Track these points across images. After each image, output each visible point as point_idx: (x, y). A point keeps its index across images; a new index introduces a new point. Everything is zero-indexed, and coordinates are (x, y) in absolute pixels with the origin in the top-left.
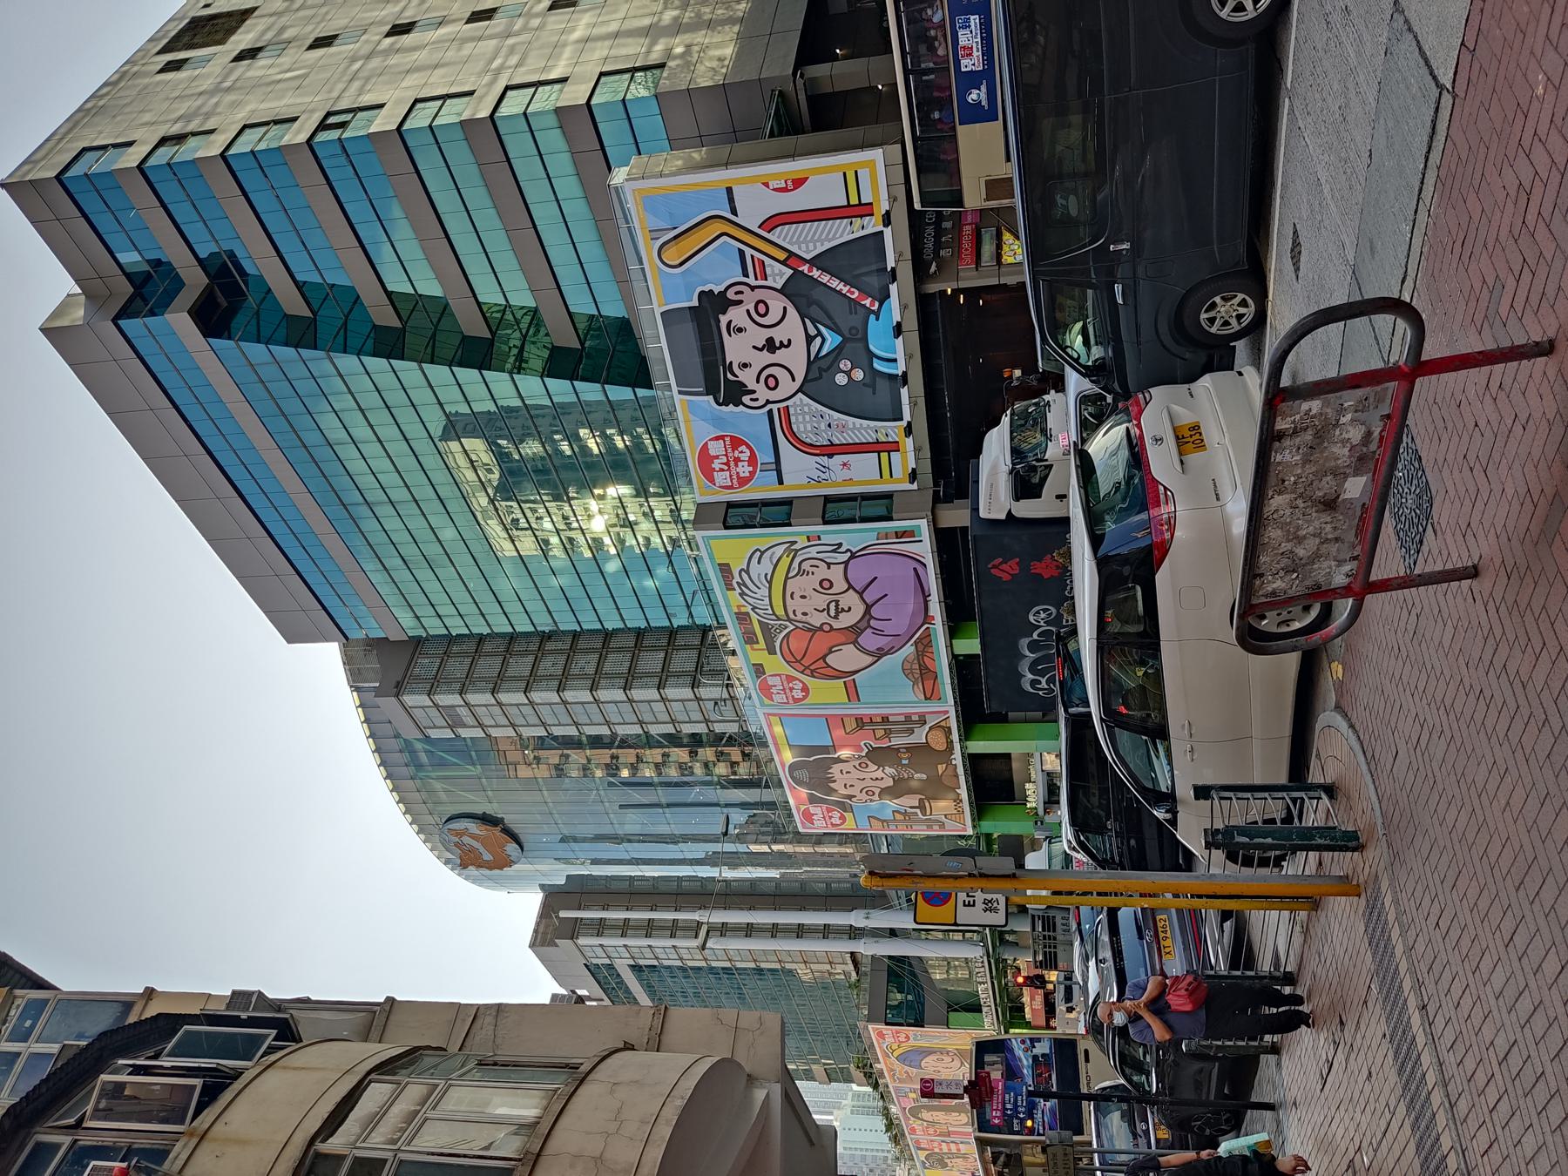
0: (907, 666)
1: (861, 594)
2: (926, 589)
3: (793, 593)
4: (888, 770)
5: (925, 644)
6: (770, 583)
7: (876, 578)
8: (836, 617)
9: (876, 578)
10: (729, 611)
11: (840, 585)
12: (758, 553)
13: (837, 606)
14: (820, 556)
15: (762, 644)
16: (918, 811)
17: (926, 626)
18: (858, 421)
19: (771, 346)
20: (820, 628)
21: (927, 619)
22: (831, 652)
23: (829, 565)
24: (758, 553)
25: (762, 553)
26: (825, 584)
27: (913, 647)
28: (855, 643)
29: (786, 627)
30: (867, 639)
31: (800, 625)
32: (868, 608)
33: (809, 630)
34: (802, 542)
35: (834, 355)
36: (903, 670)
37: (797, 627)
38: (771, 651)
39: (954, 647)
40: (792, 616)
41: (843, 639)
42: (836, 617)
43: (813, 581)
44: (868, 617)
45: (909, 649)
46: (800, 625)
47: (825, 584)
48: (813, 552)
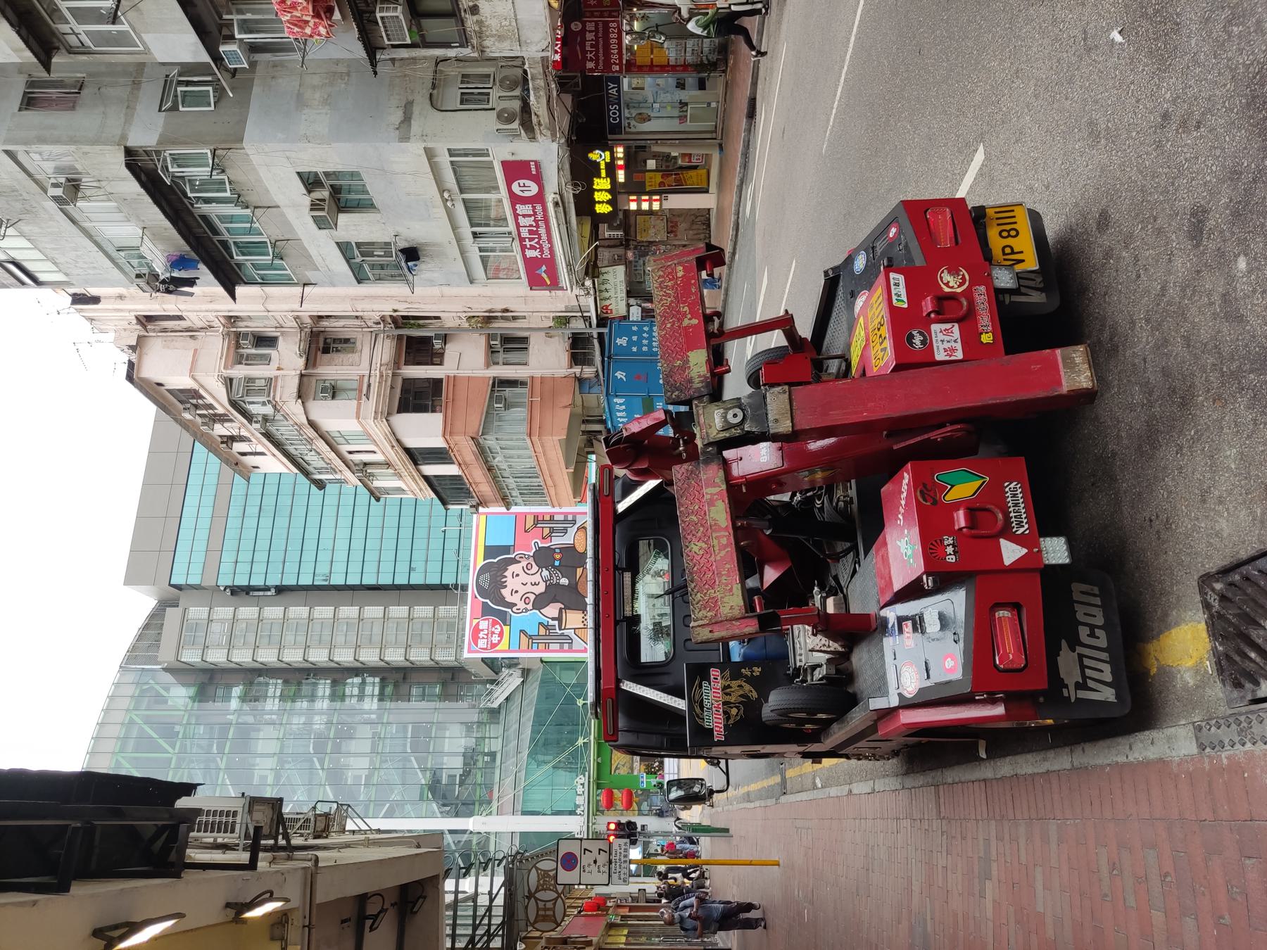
4: (546, 573)
16: (556, 623)
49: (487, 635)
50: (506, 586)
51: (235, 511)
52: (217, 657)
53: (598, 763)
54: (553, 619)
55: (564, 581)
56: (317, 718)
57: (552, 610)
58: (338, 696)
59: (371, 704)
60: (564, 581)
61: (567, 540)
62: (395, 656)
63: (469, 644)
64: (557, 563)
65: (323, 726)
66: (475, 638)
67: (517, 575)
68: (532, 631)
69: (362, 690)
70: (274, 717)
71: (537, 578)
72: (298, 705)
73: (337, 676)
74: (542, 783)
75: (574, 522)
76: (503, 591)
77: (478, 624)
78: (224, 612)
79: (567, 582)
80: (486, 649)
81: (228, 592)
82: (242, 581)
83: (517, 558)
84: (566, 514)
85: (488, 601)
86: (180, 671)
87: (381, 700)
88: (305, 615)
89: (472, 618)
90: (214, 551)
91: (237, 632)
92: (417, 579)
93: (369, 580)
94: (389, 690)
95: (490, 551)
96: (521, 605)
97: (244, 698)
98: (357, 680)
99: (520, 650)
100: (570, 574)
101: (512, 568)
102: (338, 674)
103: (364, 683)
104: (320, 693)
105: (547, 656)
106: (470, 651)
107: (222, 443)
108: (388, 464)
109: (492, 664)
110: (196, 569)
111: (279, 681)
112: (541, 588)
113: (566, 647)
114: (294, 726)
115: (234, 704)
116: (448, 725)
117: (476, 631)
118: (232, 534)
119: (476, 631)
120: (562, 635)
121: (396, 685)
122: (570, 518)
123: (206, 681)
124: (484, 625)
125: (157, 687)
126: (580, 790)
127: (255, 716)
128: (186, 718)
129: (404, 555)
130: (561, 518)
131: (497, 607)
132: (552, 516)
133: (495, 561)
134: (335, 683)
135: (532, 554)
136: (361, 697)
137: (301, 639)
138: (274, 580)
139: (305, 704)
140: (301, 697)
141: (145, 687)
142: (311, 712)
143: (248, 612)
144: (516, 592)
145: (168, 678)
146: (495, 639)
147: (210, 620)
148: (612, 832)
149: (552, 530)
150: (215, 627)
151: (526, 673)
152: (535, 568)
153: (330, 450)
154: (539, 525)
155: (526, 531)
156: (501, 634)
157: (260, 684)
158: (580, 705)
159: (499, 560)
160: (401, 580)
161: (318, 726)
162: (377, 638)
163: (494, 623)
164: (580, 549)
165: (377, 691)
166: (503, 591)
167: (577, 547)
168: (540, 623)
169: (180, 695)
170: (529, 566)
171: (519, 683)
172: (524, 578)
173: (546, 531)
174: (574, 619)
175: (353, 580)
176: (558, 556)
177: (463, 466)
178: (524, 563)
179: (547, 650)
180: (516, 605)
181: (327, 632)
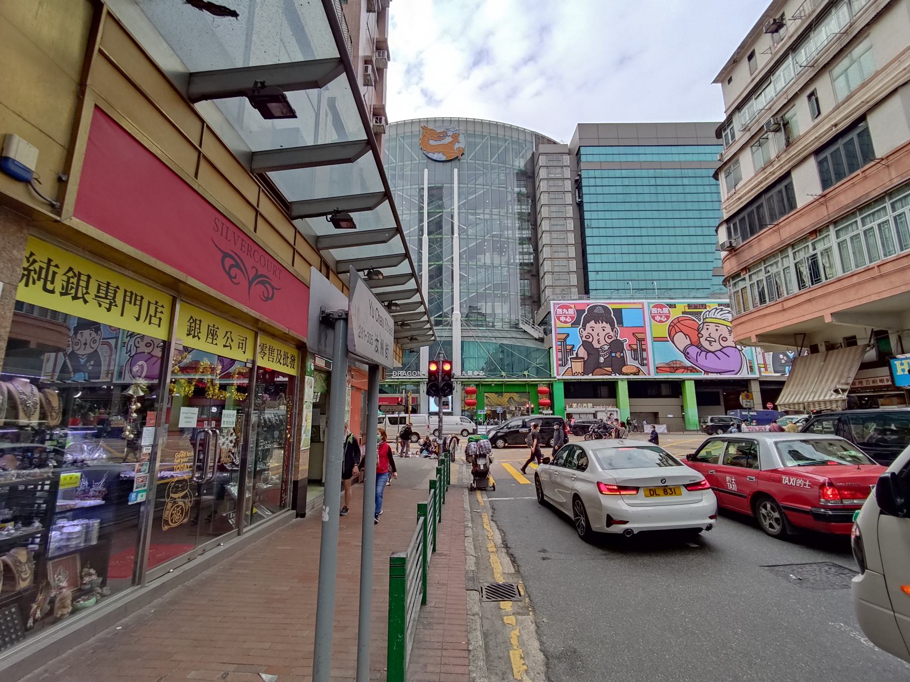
0: (677, 362)
1: (720, 350)
4: (606, 347)
5: (692, 370)
6: (724, 320)
8: (706, 340)
10: (708, 302)
11: (724, 344)
15: (687, 310)
16: (575, 356)
17: (703, 372)
18: (771, 359)
20: (699, 333)
21: (707, 372)
22: (685, 335)
28: (692, 345)
30: (693, 351)
31: (701, 326)
32: (713, 352)
33: (698, 329)
36: (676, 361)
37: (700, 325)
38: (683, 313)
43: (726, 334)
45: (688, 364)
46: (701, 326)
49: (565, 314)
50: (596, 323)
51: (625, 173)
52: (543, 173)
53: (490, 385)
54: (577, 354)
55: (602, 360)
56: (510, 232)
57: (583, 353)
58: (522, 241)
59: (518, 259)
60: (602, 360)
61: (630, 361)
62: (547, 266)
63: (559, 304)
64: (613, 354)
65: (506, 236)
66: (562, 307)
67: (604, 330)
68: (569, 341)
69: (526, 253)
70: (511, 211)
71: (603, 342)
72: (517, 222)
73: (533, 240)
74: (479, 353)
75: (643, 365)
76: (593, 322)
77: (571, 308)
78: (567, 173)
79: (602, 362)
80: (556, 314)
81: (577, 178)
82: (584, 182)
83: (615, 329)
85: (586, 313)
86: (533, 160)
87: (521, 264)
88: (568, 215)
89: (575, 305)
90: (601, 166)
91: (556, 182)
92: (591, 276)
93: (589, 249)
94: (525, 268)
95: (618, 312)
96: (585, 333)
97: (519, 194)
98: (531, 250)
99: (557, 334)
100: (606, 364)
101: (608, 326)
102: (534, 241)
103: (531, 254)
104: (524, 232)
105: (554, 352)
106: (554, 304)
107: (775, 20)
108: (789, 144)
109: (545, 322)
110: (590, 158)
111: (529, 211)
112: (596, 345)
113: (560, 362)
114: (506, 221)
115: (516, 190)
116: (509, 304)
117: (567, 307)
118: (612, 173)
119: (567, 307)
120: (567, 360)
121: (529, 271)
123: (528, 174)
124: (571, 312)
125: (524, 151)
126: (476, 373)
127: (511, 201)
128: (509, 166)
129: (606, 267)
130: (645, 356)
131: (583, 318)
132: (644, 350)
133: (612, 316)
134: (529, 239)
135: (618, 338)
136: (522, 253)
137: (554, 215)
138: (586, 199)
139: (517, 225)
140: (522, 222)
141: (524, 145)
142: (513, 229)
143: (568, 185)
144: (593, 330)
145: (529, 155)
146: (563, 319)
147: (562, 167)
148: (441, 368)
149: (635, 350)
150: (559, 170)
151: (541, 340)
152: (609, 341)
153: (789, 98)
156: (565, 322)
157: (528, 201)
158: (525, 373)
159: (614, 317)
160: (590, 267)
161: (506, 233)
162: (556, 255)
163: (572, 318)
164: (624, 370)
165: (526, 261)
166: (593, 322)
167: (625, 367)
168: (574, 346)
169: (520, 163)
170: (610, 337)
171: (535, 336)
172: (602, 334)
173: (635, 347)
174: (578, 367)
175: (589, 241)
176: (618, 355)
177: (823, 199)
178: (612, 334)
179: (558, 351)
180: (585, 330)
181: (559, 228)
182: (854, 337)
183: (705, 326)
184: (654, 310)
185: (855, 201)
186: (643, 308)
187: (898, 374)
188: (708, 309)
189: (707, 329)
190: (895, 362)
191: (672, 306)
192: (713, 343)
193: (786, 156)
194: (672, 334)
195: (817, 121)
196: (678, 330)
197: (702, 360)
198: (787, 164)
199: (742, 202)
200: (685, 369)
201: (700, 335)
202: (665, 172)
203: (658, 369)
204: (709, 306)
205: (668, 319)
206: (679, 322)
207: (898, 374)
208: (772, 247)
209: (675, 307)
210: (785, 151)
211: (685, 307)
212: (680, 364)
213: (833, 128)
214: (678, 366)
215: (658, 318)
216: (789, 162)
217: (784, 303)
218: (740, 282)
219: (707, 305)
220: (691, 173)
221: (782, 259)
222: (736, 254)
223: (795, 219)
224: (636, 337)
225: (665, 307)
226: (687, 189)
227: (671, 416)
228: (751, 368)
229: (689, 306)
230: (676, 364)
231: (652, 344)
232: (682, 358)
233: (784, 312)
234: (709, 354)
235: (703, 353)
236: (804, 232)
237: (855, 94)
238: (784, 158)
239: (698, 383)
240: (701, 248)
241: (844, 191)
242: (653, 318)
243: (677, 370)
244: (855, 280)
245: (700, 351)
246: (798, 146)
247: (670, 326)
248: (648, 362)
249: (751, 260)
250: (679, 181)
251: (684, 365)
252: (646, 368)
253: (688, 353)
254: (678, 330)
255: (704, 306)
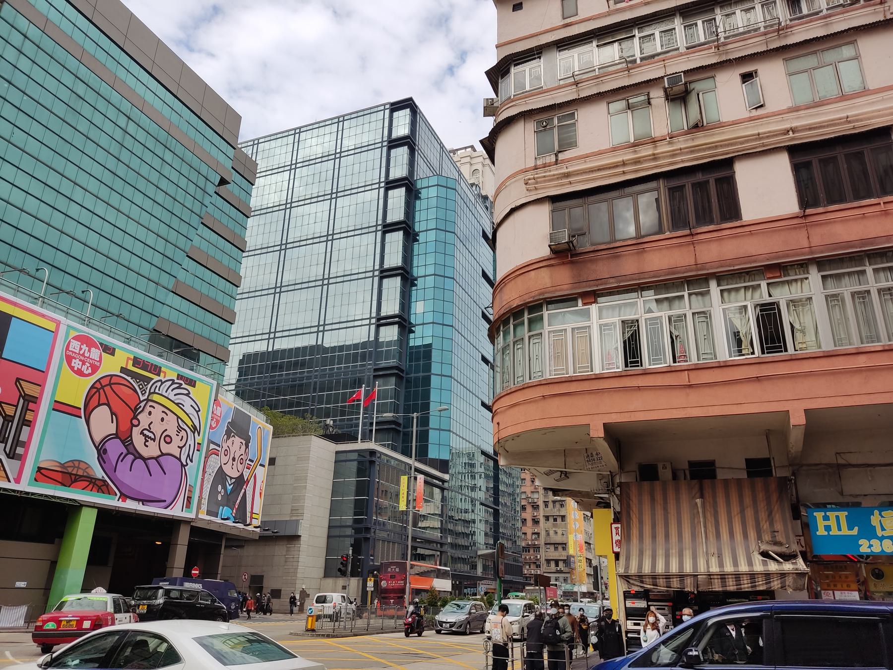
0: (82, 466)
1: (156, 458)
2: (149, 504)
3: (154, 408)
5: (101, 487)
6: (177, 404)
7: (165, 474)
8: (142, 433)
9: (165, 474)
10: (167, 367)
11: (166, 448)
12: (197, 409)
13: (152, 439)
14: (187, 445)
17: (119, 494)
19: (234, 459)
20: (135, 417)
21: (124, 497)
22: (112, 413)
23: (181, 448)
24: (197, 409)
25: (197, 412)
26: (168, 440)
27: (100, 477)
28: (117, 436)
29: (143, 394)
30: (115, 448)
31: (142, 405)
32: (145, 460)
34: (199, 439)
35: (100, 458)
36: (80, 461)
37: (141, 402)
38: (123, 370)
39: (90, 509)
40: (151, 403)
41: (122, 429)
42: (142, 433)
43: (172, 432)
44: (137, 456)
45: (99, 473)
46: (142, 405)
47: (168, 440)
48: (191, 442)
75: (11, 455)
84: (26, 445)
118: (60, 53)
122: (20, 450)
130: (23, 437)
154: (21, 401)
155: (18, 380)
182: (712, 463)
183: (148, 406)
184: (75, 345)
185: (864, 241)
186: (55, 333)
187: (818, 533)
188: (161, 377)
189: (150, 413)
190: (815, 514)
191: (109, 350)
192: (150, 443)
193: (687, 140)
194: (91, 406)
195: (755, 113)
196: (103, 400)
197: (124, 473)
198: (687, 153)
199: (624, 173)
200: (91, 482)
201: (135, 422)
202: (145, 121)
203: (42, 474)
204: (165, 373)
205: (94, 372)
206: (110, 384)
207: (818, 533)
208: (672, 271)
209: (113, 354)
210: (686, 133)
211: (128, 359)
212: (84, 470)
213: (791, 133)
214: (80, 473)
215: (76, 364)
216: (692, 152)
217: (692, 374)
218: (568, 316)
219: (163, 369)
220: (179, 150)
221: (690, 295)
222: (572, 262)
223: (735, 236)
224: (19, 388)
225: (97, 348)
226: (166, 170)
227: (21, 584)
228: (189, 498)
229: (137, 362)
230: (78, 468)
231: (48, 414)
232: (91, 457)
233: (688, 390)
234: (139, 461)
235: (130, 457)
236: (755, 261)
237: (828, 104)
238: (682, 143)
239: (104, 515)
240: (154, 274)
241: (845, 220)
242: (69, 359)
243: (76, 481)
244: (862, 361)
245: (125, 451)
246: (723, 133)
247: (92, 387)
248: (26, 452)
249: (612, 280)
250: (159, 150)
251: (91, 473)
252: (16, 463)
253: (105, 451)
254: (103, 400)
255: (157, 370)
